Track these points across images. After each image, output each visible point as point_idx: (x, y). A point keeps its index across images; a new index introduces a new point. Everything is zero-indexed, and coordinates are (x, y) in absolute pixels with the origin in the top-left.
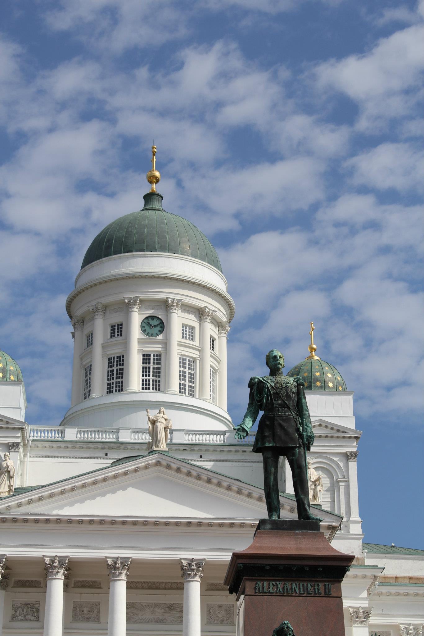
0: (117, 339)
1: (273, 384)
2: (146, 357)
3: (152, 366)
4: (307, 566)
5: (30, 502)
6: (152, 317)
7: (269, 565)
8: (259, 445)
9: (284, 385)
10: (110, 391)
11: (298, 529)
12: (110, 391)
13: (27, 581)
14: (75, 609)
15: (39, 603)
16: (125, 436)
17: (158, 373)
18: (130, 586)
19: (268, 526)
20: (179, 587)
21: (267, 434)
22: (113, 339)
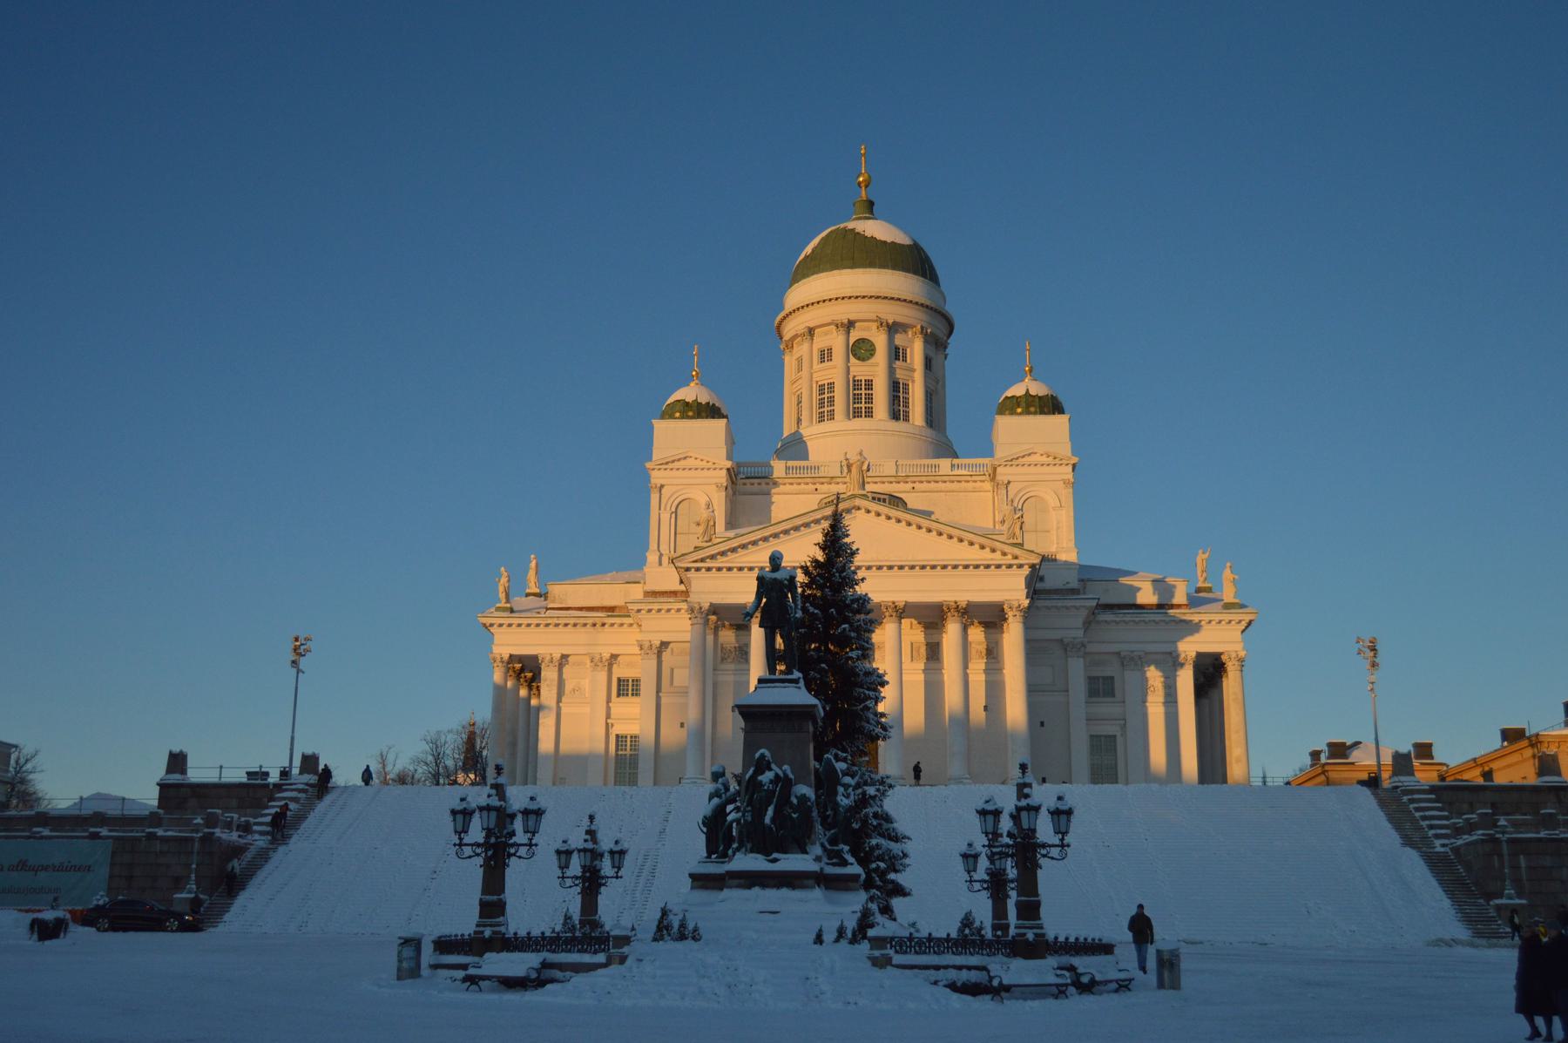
0: (826, 364)
5: (733, 550)
6: (863, 340)
12: (821, 420)
17: (869, 399)
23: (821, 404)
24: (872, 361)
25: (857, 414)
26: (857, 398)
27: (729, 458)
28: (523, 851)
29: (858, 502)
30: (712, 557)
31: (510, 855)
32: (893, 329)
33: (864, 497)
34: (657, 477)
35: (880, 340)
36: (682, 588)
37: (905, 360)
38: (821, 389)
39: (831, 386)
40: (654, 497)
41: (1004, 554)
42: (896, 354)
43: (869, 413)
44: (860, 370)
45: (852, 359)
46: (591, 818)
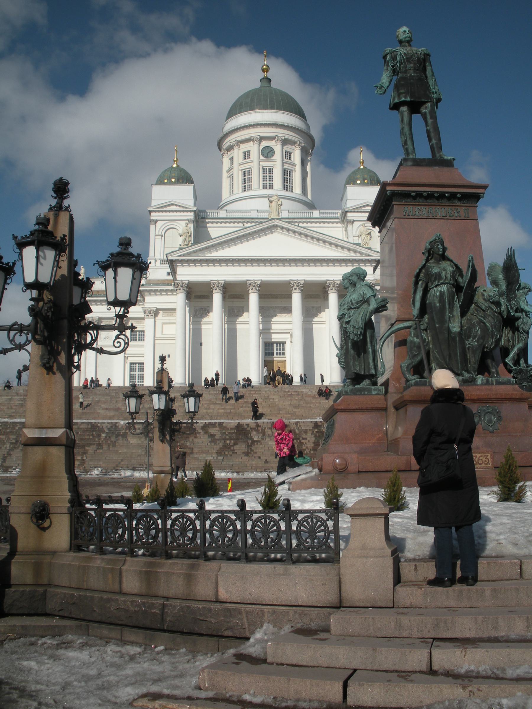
0: (247, 160)
1: (405, 52)
2: (264, 170)
3: (268, 175)
4: (447, 192)
7: (414, 192)
8: (396, 101)
9: (415, 52)
10: (244, 190)
11: (436, 165)
12: (244, 190)
13: (201, 295)
14: (229, 311)
15: (209, 307)
16: (254, 215)
17: (271, 179)
18: (262, 297)
19: (410, 163)
20: (290, 297)
21: (402, 91)
22: (245, 161)
23: (244, 181)
24: (273, 158)
25: (265, 187)
26: (264, 179)
27: (195, 205)
28: (106, 339)
29: (277, 222)
30: (189, 254)
31: (82, 347)
32: (285, 142)
33: (280, 219)
34: (154, 216)
35: (277, 148)
36: (170, 277)
37: (290, 159)
38: (244, 174)
39: (250, 172)
40: (152, 227)
41: (361, 253)
42: (288, 155)
43: (271, 187)
44: (267, 164)
45: (262, 158)
46: (163, 359)
